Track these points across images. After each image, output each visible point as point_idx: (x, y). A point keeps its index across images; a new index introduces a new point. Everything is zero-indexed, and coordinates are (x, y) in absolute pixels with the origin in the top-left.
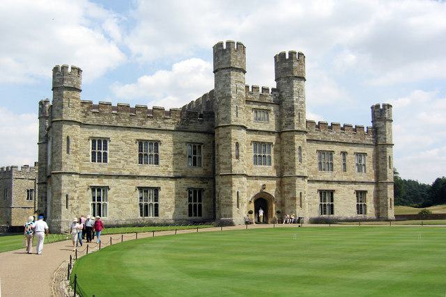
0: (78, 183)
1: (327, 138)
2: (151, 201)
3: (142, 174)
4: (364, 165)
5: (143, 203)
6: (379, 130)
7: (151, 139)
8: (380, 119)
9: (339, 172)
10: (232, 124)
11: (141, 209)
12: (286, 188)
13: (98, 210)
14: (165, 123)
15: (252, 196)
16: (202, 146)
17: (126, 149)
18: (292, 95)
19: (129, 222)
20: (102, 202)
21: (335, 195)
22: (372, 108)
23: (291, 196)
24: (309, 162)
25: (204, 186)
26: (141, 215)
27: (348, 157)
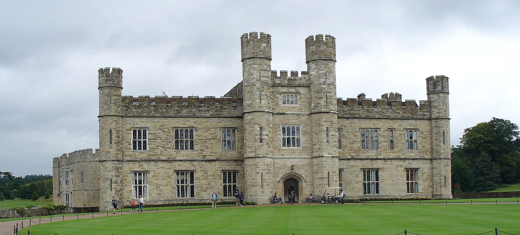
0: (121, 168)
1: (371, 115)
2: (189, 183)
3: (178, 158)
4: (416, 141)
5: (180, 185)
6: (432, 104)
7: (186, 126)
8: (434, 93)
9: (385, 150)
10: (257, 110)
11: (178, 191)
12: (315, 167)
13: (140, 191)
14: (199, 111)
15: (280, 176)
16: (236, 130)
19: (167, 203)
20: (143, 185)
21: (380, 173)
22: (428, 80)
23: (319, 175)
24: (351, 140)
26: (179, 196)
27: (396, 134)
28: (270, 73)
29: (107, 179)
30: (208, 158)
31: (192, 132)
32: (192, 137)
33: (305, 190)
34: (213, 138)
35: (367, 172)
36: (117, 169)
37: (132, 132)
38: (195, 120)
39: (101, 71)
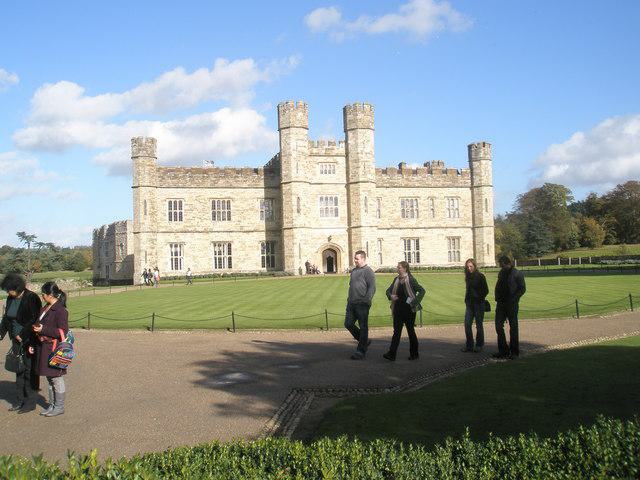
1: (410, 184)
5: (218, 256)
12: (353, 238)
13: (176, 264)
17: (199, 207)
18: (357, 145)
20: (179, 257)
25: (276, 239)
27: (436, 202)
28: (306, 144)
29: (140, 251)
30: (246, 229)
31: (229, 202)
32: (229, 207)
33: (344, 264)
34: (251, 209)
35: (407, 243)
36: (152, 241)
37: (167, 203)
38: (232, 190)
39: (134, 141)
